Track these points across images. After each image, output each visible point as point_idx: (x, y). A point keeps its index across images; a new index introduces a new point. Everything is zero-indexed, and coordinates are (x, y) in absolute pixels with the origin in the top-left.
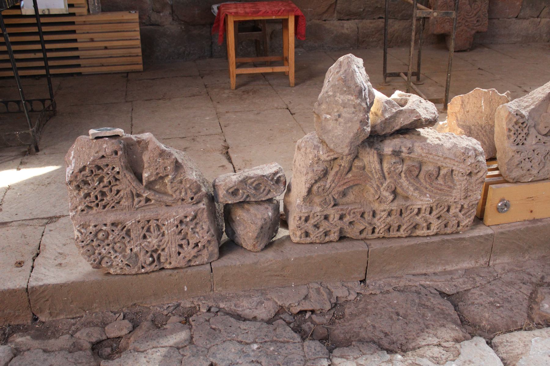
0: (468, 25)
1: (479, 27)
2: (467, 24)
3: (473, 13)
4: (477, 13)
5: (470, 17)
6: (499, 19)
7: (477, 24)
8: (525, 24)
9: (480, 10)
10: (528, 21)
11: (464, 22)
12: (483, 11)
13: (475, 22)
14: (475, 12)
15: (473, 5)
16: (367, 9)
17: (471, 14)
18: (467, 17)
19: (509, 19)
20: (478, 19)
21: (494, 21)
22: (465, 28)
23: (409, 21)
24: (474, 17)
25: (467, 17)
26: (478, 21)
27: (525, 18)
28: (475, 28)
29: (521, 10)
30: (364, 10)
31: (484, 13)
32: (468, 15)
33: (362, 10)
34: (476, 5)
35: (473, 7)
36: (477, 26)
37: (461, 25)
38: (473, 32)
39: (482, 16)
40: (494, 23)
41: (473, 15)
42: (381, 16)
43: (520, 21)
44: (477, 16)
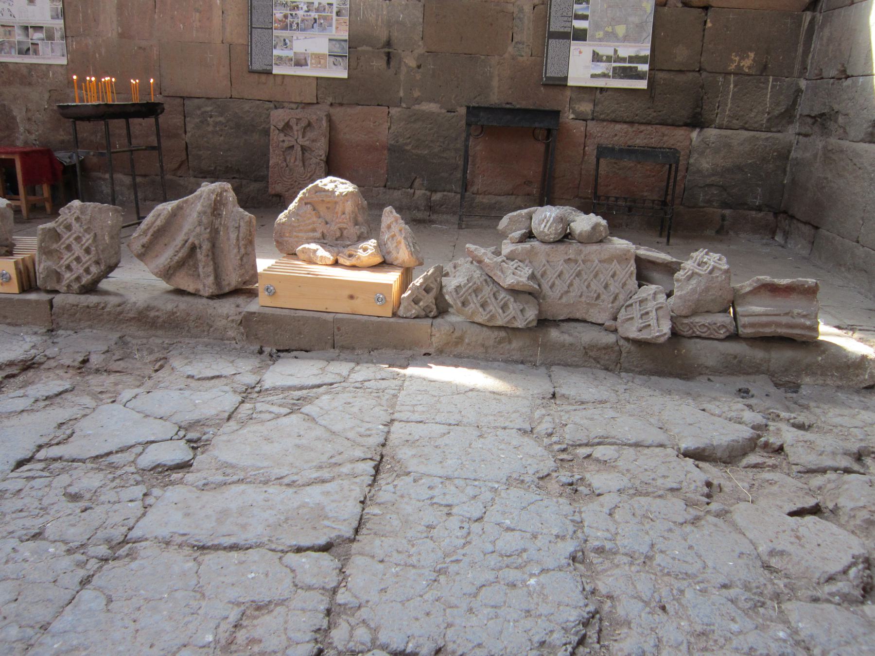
4: (311, 176)
10: (400, 192)
11: (297, 183)
14: (309, 175)
16: (218, 168)
19: (377, 187)
27: (395, 189)
30: (215, 168)
33: (213, 168)
42: (235, 176)
43: (391, 191)
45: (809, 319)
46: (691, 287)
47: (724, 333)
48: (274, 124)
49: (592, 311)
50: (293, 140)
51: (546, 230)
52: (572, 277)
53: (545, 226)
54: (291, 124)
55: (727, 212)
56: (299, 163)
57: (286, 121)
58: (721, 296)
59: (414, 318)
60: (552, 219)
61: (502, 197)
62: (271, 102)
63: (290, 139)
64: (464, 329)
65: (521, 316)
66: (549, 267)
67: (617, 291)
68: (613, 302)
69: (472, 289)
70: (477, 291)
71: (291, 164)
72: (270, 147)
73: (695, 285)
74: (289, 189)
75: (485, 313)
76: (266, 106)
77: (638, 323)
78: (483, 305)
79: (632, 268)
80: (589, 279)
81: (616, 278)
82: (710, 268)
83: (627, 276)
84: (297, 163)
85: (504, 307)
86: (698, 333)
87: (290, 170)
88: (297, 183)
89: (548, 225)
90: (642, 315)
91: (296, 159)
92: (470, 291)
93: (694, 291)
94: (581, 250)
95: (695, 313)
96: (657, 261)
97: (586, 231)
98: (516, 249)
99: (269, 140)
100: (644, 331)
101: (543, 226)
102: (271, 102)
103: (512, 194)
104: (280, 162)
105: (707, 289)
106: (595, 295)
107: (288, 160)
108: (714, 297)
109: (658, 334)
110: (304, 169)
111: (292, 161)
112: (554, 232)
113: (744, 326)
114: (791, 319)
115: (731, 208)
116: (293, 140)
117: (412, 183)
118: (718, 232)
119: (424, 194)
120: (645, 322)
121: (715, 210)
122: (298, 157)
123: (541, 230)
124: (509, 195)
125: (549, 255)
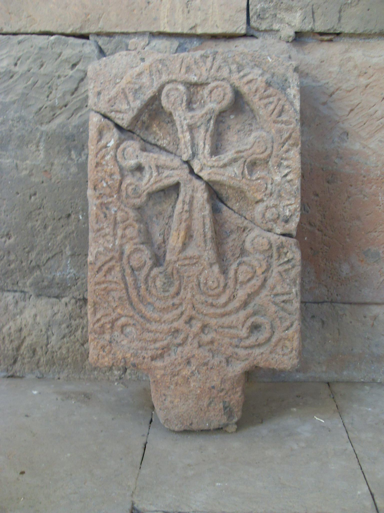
0: (212, 342)
1: (262, 350)
2: (206, 338)
3: (233, 297)
4: (251, 296)
5: (219, 311)
7: (252, 341)
9: (263, 285)
11: (197, 325)
12: (279, 289)
13: (244, 332)
14: (242, 294)
15: (234, 267)
17: (223, 299)
20: (258, 319)
22: (203, 353)
23: (64, 300)
24: (237, 310)
26: (255, 327)
28: (242, 352)
32: (212, 305)
34: (243, 268)
35: (231, 273)
36: (252, 347)
37: (186, 338)
39: (273, 308)
40: (375, 318)
41: (236, 304)
44: (249, 309)
48: (103, 107)
50: (177, 162)
54: (164, 102)
57: (149, 93)
62: (85, 37)
63: (164, 158)
72: (90, 192)
74: (166, 349)
76: (67, 53)
84: (191, 251)
87: (169, 277)
88: (197, 325)
99: (83, 167)
102: (85, 37)
104: (128, 249)
107: (158, 238)
110: (224, 271)
116: (177, 162)
122: (197, 226)
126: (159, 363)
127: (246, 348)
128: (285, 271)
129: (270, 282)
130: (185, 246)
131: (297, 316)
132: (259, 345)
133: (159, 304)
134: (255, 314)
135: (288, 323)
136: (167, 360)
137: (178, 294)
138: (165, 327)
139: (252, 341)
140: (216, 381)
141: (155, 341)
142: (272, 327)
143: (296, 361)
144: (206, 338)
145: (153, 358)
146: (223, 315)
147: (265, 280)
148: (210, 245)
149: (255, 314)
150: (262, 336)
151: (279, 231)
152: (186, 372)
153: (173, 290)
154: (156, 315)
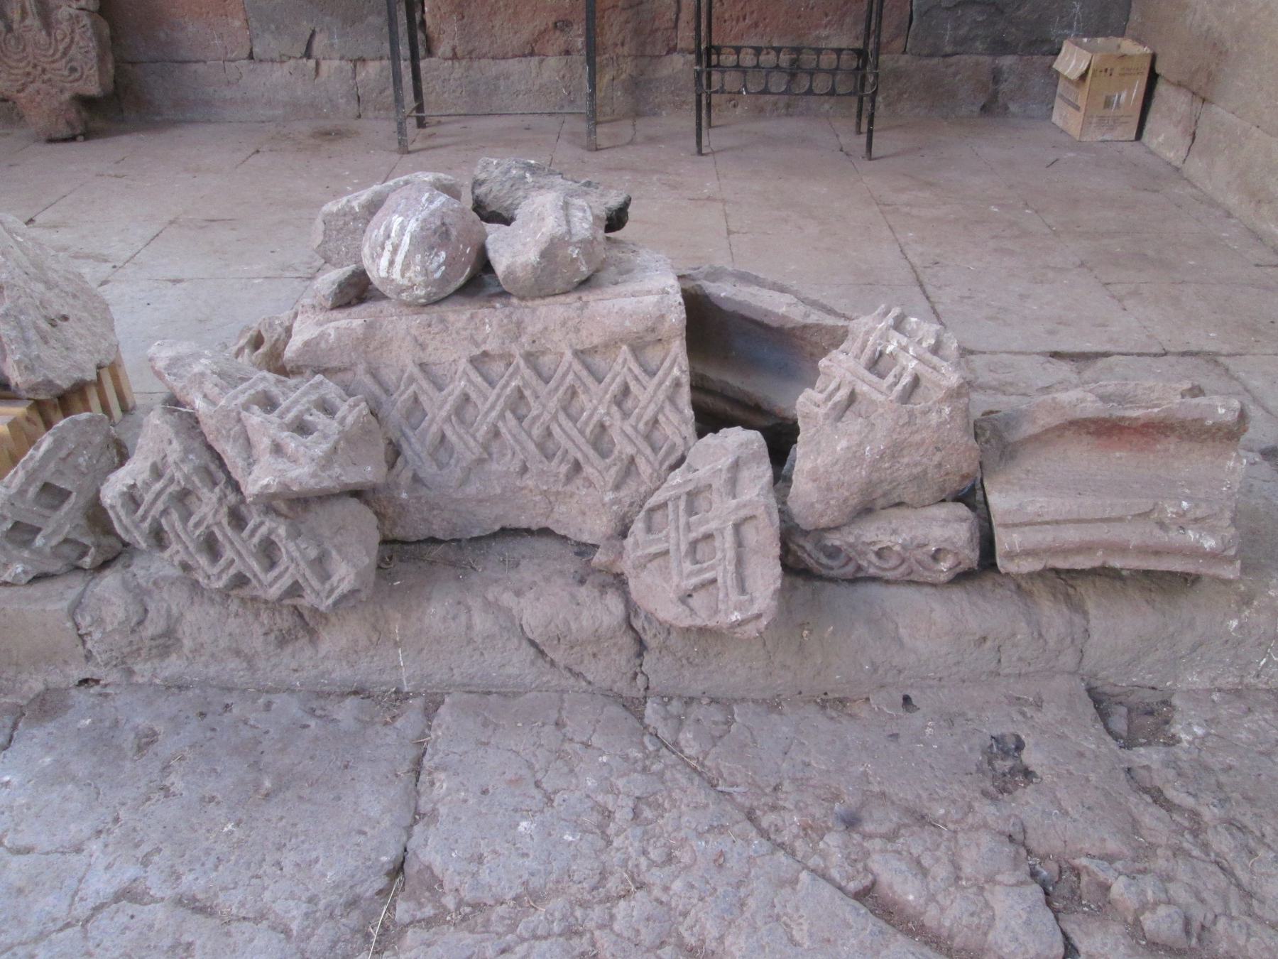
0: (50, 80)
2: (46, 77)
3: (56, 50)
5: (50, 59)
6: (205, 62)
8: (279, 74)
9: (72, 41)
11: (39, 68)
12: (81, 44)
13: (66, 73)
14: (61, 47)
18: (42, 59)
20: (74, 64)
21: (194, 67)
24: (62, 58)
25: (42, 59)
26: (73, 70)
28: (68, 85)
29: (251, 40)
31: (83, 50)
32: (45, 56)
38: (67, 96)
39: (79, 57)
40: (195, 71)
41: (59, 55)
43: (267, 67)
45: (1212, 531)
46: (843, 443)
47: (950, 569)
49: (563, 509)
51: (396, 274)
52: (494, 414)
53: (392, 263)
55: (1007, 61)
56: (33, 21)
58: (939, 465)
59: (30, 582)
60: (407, 239)
61: (511, 61)
64: (175, 610)
65: (315, 583)
66: (425, 385)
67: (630, 450)
68: (617, 487)
69: (164, 497)
70: (183, 497)
71: (15, 26)
73: (856, 439)
75: (215, 570)
77: (683, 574)
78: (211, 546)
79: (676, 372)
80: (546, 416)
81: (629, 404)
82: (906, 380)
83: (661, 396)
84: (28, 22)
85: (268, 552)
86: (872, 571)
88: (39, 68)
89: (399, 258)
90: (694, 545)
91: (24, 13)
92: (160, 506)
93: (855, 456)
94: (519, 324)
95: (866, 511)
96: (766, 321)
97: (525, 266)
98: (322, 336)
100: (696, 601)
101: (384, 262)
103: (532, 54)
105: (895, 451)
106: (564, 469)
108: (919, 469)
109: (736, 616)
110: (49, 34)
111: (16, 16)
112: (420, 279)
113: (1011, 556)
114: (1158, 532)
115: (1014, 53)
117: (309, 45)
118: (985, 109)
119: (340, 70)
120: (700, 571)
121: (981, 59)
123: (383, 274)
124: (524, 56)
125: (423, 347)
126: (22, 95)
127: (71, 82)
128: (84, 32)
129: (76, 39)
130: (23, 18)
131: (95, 60)
132: (77, 80)
133: (16, 57)
134: (71, 60)
135: (89, 66)
136: (27, 91)
137: (24, 50)
138: (20, 72)
139: (71, 78)
140: (57, 104)
141: (17, 81)
142: (82, 68)
143: (99, 90)
144: (46, 77)
145: (18, 91)
146: (53, 62)
147: (72, 41)
148: (37, 18)
149: (71, 60)
150: (77, 75)
151: (75, 6)
152: (38, 99)
153: (21, 47)
154: (14, 64)
